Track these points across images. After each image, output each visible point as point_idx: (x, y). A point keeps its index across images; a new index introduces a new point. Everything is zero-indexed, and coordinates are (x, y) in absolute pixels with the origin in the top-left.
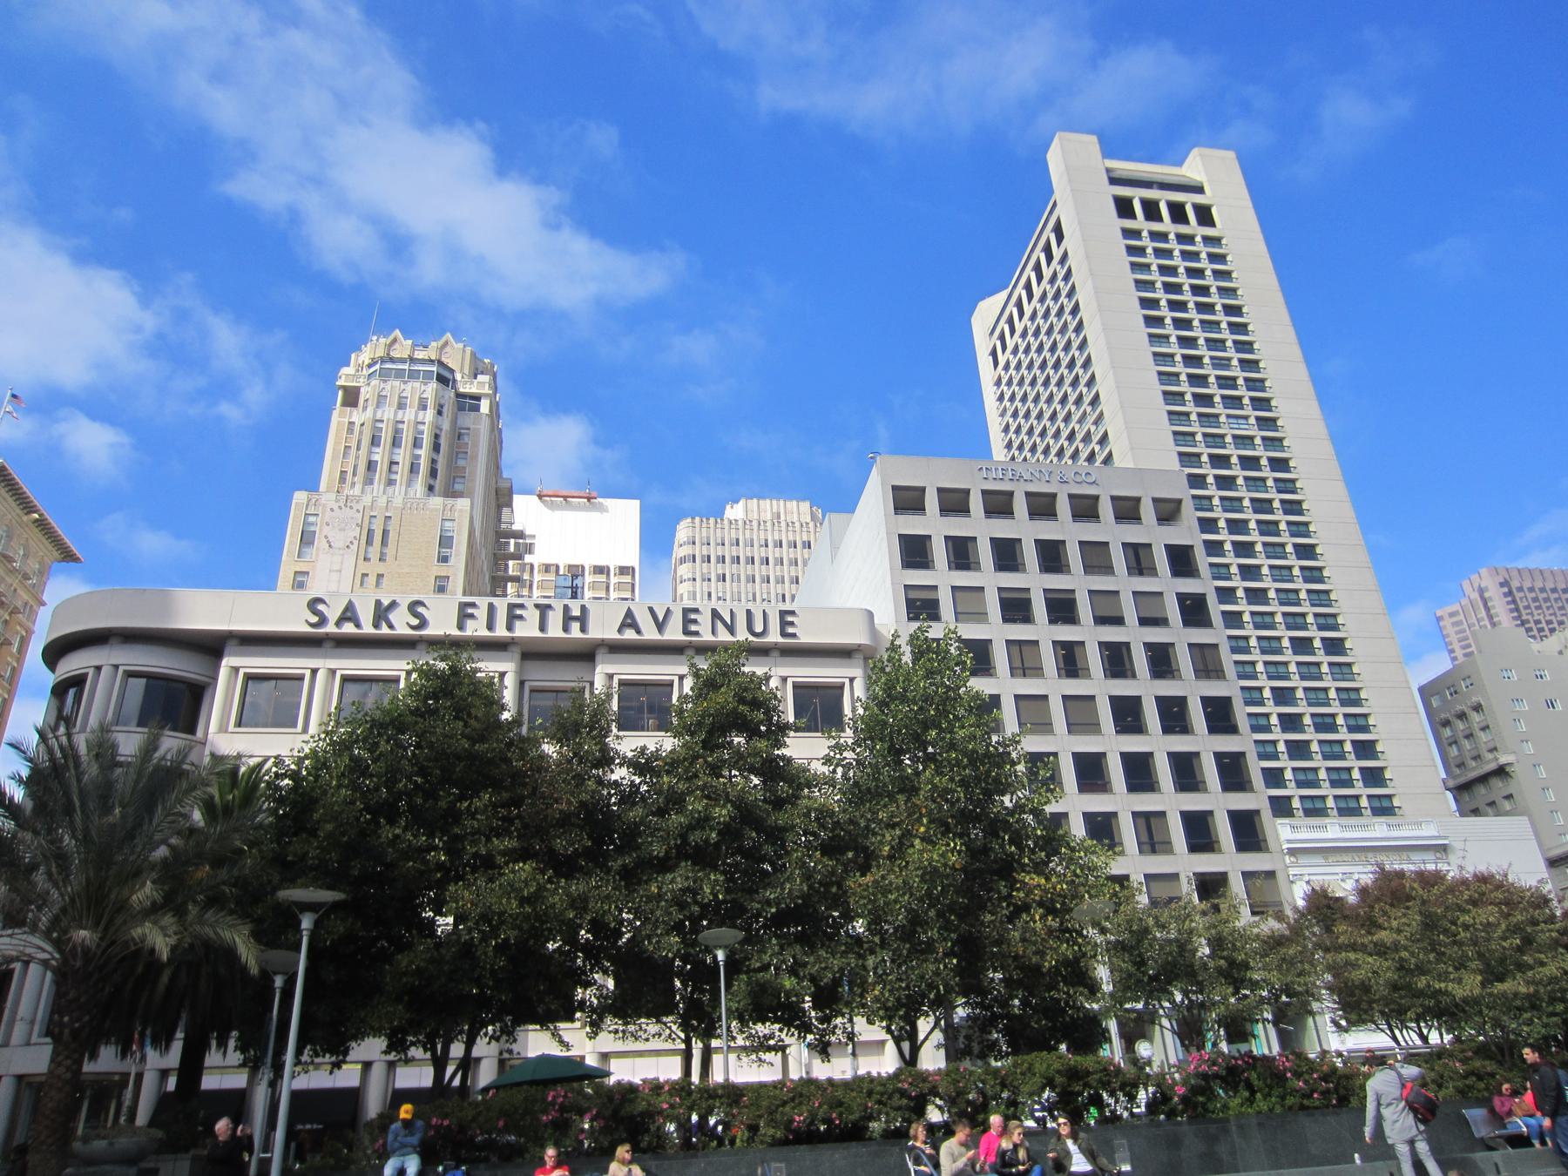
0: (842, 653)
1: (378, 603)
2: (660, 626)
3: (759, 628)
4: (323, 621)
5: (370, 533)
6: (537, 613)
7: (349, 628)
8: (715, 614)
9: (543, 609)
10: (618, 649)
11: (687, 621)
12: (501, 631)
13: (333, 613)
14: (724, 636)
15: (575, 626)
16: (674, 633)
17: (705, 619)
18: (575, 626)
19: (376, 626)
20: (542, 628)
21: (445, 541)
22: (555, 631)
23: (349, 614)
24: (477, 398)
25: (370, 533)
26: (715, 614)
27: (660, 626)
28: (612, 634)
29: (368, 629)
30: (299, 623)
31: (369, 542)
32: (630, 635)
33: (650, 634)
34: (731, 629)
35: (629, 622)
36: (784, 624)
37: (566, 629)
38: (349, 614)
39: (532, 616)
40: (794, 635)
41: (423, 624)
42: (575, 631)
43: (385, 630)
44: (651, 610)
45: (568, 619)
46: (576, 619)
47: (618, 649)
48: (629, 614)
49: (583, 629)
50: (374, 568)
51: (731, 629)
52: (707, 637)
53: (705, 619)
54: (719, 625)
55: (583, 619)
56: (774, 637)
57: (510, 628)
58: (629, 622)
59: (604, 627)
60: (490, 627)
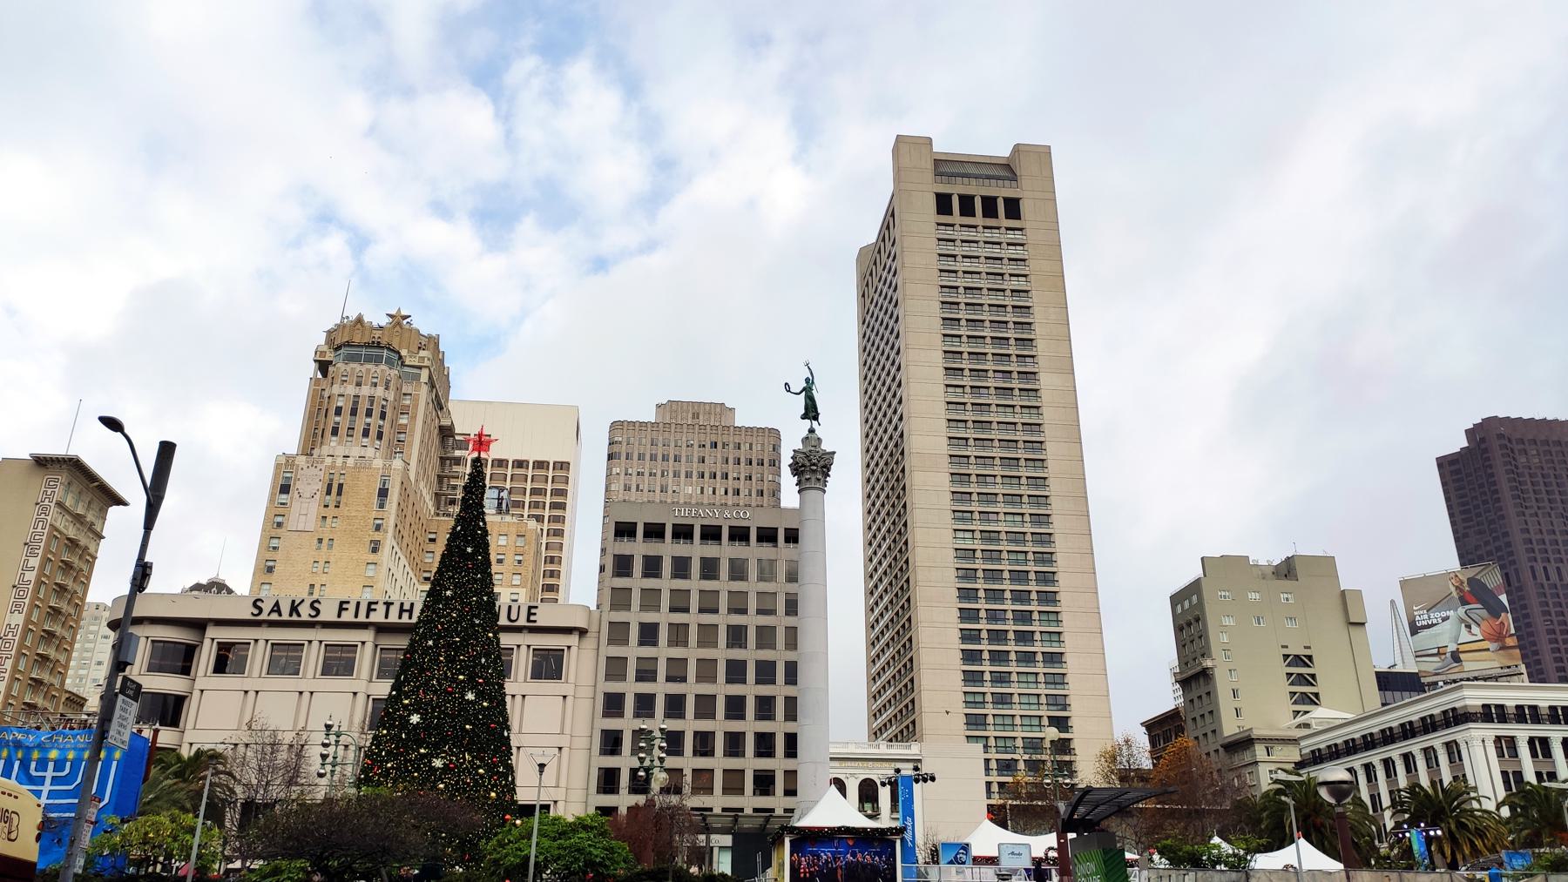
0: (568, 631)
3: (513, 617)
4: (261, 610)
5: (330, 487)
7: (274, 616)
9: (388, 604)
12: (362, 618)
13: (267, 606)
15: (406, 615)
18: (406, 615)
21: (383, 493)
23: (276, 608)
24: (420, 368)
29: (285, 617)
30: (246, 613)
31: (329, 492)
36: (530, 614)
38: (276, 608)
39: (381, 608)
41: (318, 612)
43: (295, 618)
45: (402, 611)
56: (522, 622)
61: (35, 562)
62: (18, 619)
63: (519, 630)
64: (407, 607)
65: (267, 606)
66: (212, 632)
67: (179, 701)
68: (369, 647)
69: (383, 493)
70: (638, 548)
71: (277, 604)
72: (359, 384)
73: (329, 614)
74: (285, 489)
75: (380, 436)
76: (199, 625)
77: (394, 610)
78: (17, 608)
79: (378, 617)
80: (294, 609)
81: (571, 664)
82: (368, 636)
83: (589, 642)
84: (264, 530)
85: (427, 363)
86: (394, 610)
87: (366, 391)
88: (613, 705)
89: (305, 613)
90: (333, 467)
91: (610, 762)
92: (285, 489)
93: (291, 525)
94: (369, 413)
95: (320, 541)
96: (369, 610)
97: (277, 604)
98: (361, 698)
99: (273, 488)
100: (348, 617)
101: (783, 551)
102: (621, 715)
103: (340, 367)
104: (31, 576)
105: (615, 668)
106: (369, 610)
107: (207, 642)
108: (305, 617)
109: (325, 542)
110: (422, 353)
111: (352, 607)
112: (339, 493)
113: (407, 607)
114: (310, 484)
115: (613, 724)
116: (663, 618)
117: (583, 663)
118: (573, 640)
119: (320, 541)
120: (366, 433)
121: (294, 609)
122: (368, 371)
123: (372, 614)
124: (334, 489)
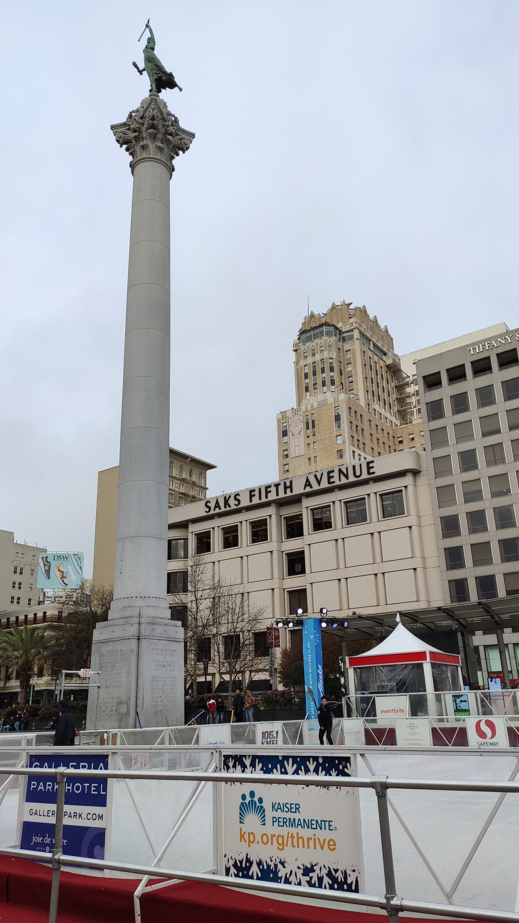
0: (402, 474)
1: (225, 498)
2: (319, 482)
3: (358, 474)
4: (210, 508)
5: (307, 424)
6: (275, 488)
7: (217, 511)
8: (340, 471)
10: (309, 495)
11: (329, 477)
12: (264, 500)
13: (212, 505)
14: (344, 481)
15: (288, 490)
16: (325, 484)
17: (336, 474)
18: (288, 490)
19: (225, 507)
20: (277, 495)
22: (282, 495)
23: (217, 505)
24: (352, 330)
25: (307, 424)
26: (340, 471)
27: (319, 482)
28: (302, 491)
29: (223, 509)
31: (308, 428)
32: (308, 489)
33: (316, 487)
34: (347, 477)
35: (308, 483)
36: (369, 468)
37: (285, 493)
38: (217, 505)
39: (273, 489)
40: (374, 473)
41: (239, 501)
42: (289, 494)
43: (228, 509)
44: (316, 476)
45: (286, 488)
46: (288, 487)
48: (308, 480)
49: (291, 491)
50: (312, 439)
51: (347, 477)
52: (337, 483)
53: (336, 474)
54: (342, 476)
55: (291, 487)
56: (365, 476)
57: (267, 497)
59: (298, 489)
60: (260, 499)
64: (288, 484)
68: (274, 518)
69: (338, 418)
71: (217, 502)
73: (245, 502)
74: (285, 433)
75: (333, 383)
77: (281, 488)
79: (272, 496)
81: (409, 499)
83: (422, 480)
84: (279, 462)
85: (355, 325)
86: (281, 488)
87: (318, 357)
88: (450, 526)
89: (232, 502)
90: (307, 411)
91: (457, 574)
92: (285, 433)
93: (291, 455)
94: (323, 371)
95: (309, 459)
96: (267, 492)
97: (217, 502)
99: (279, 435)
100: (256, 500)
102: (458, 534)
103: (302, 347)
105: (444, 494)
106: (267, 492)
107: (190, 534)
108: (233, 507)
109: (312, 459)
110: (351, 320)
111: (257, 493)
112: (313, 427)
113: (288, 484)
114: (297, 427)
115: (453, 542)
116: (478, 443)
118: (408, 480)
119: (309, 459)
120: (324, 384)
122: (317, 344)
123: (269, 494)
124: (310, 425)
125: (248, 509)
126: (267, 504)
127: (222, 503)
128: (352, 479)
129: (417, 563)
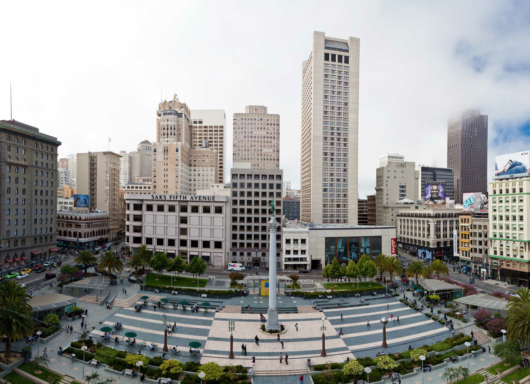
0: (223, 202)
10: (190, 201)
12: (175, 199)
13: (155, 197)
14: (204, 200)
16: (198, 199)
22: (182, 199)
23: (157, 197)
33: (194, 200)
35: (192, 198)
38: (157, 197)
39: (179, 197)
42: (185, 200)
47: (190, 201)
56: (212, 200)
58: (192, 198)
61: (108, 175)
62: (108, 188)
63: (211, 202)
65: (155, 197)
66: (145, 202)
67: (141, 216)
68: (178, 205)
70: (238, 181)
72: (168, 121)
73: (168, 198)
76: (142, 200)
78: (107, 186)
79: (179, 199)
80: (160, 197)
82: (177, 203)
83: (228, 205)
88: (234, 219)
98: (177, 217)
100: (172, 199)
101: (275, 182)
104: (108, 178)
105: (234, 211)
117: (227, 210)
118: (224, 204)
121: (160, 197)
125: (168, 201)
126: (176, 201)
127: (159, 197)
128: (207, 200)
129: (224, 228)
